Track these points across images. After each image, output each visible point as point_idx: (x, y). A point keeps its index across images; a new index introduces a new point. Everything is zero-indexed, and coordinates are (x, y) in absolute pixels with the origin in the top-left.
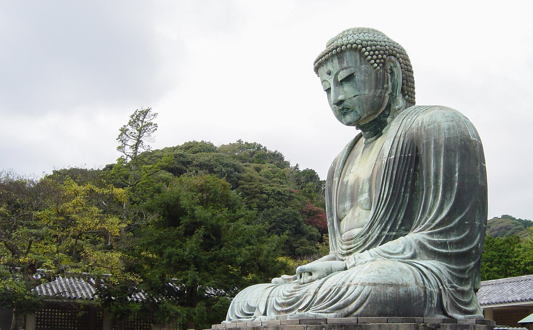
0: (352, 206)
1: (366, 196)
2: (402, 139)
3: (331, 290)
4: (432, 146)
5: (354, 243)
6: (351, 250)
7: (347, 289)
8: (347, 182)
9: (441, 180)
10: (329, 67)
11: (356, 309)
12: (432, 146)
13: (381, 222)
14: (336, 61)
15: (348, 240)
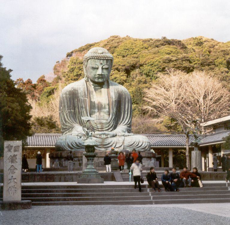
0: (98, 111)
1: (108, 110)
2: (117, 94)
3: (134, 143)
4: (127, 99)
5: (105, 125)
6: (104, 127)
7: (143, 143)
8: (94, 102)
9: (129, 110)
10: (102, 61)
11: (147, 149)
12: (127, 99)
13: (113, 120)
14: (105, 61)
15: (99, 124)
